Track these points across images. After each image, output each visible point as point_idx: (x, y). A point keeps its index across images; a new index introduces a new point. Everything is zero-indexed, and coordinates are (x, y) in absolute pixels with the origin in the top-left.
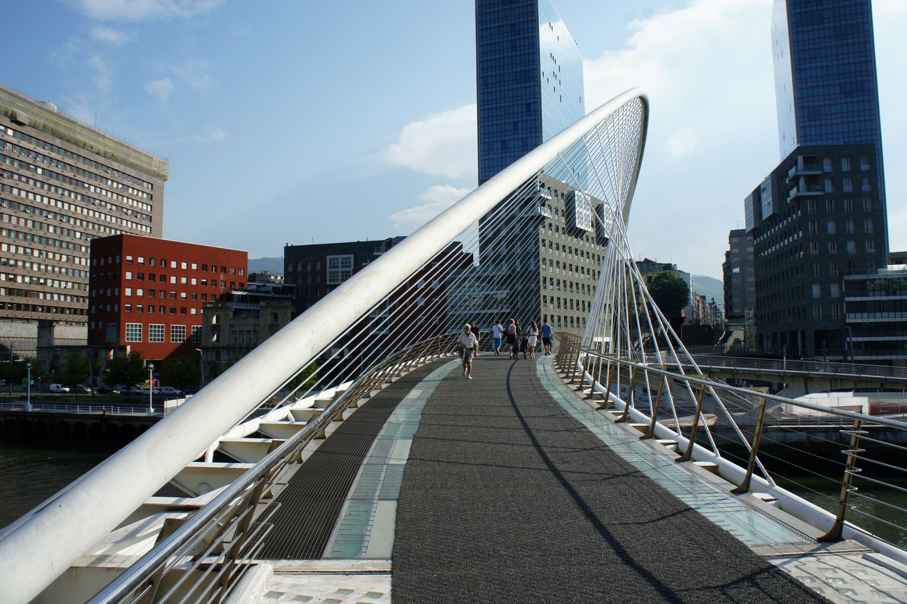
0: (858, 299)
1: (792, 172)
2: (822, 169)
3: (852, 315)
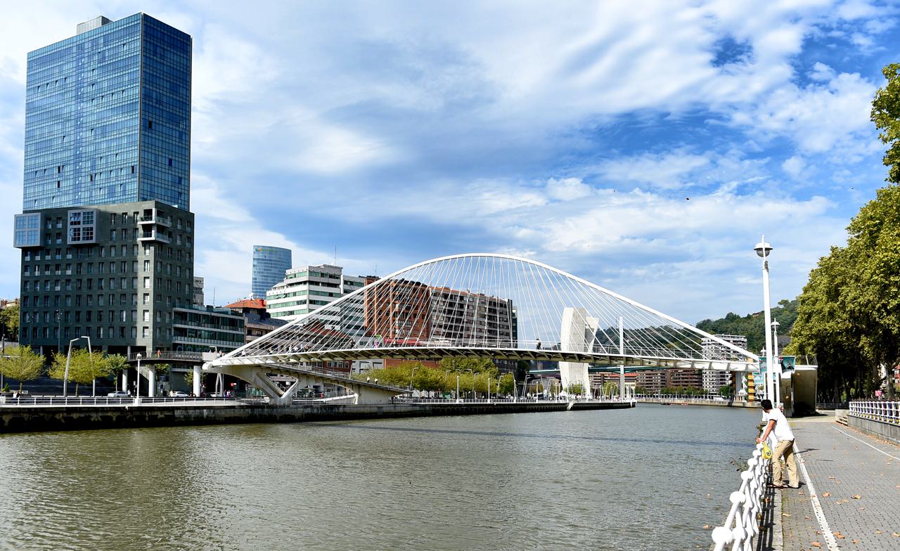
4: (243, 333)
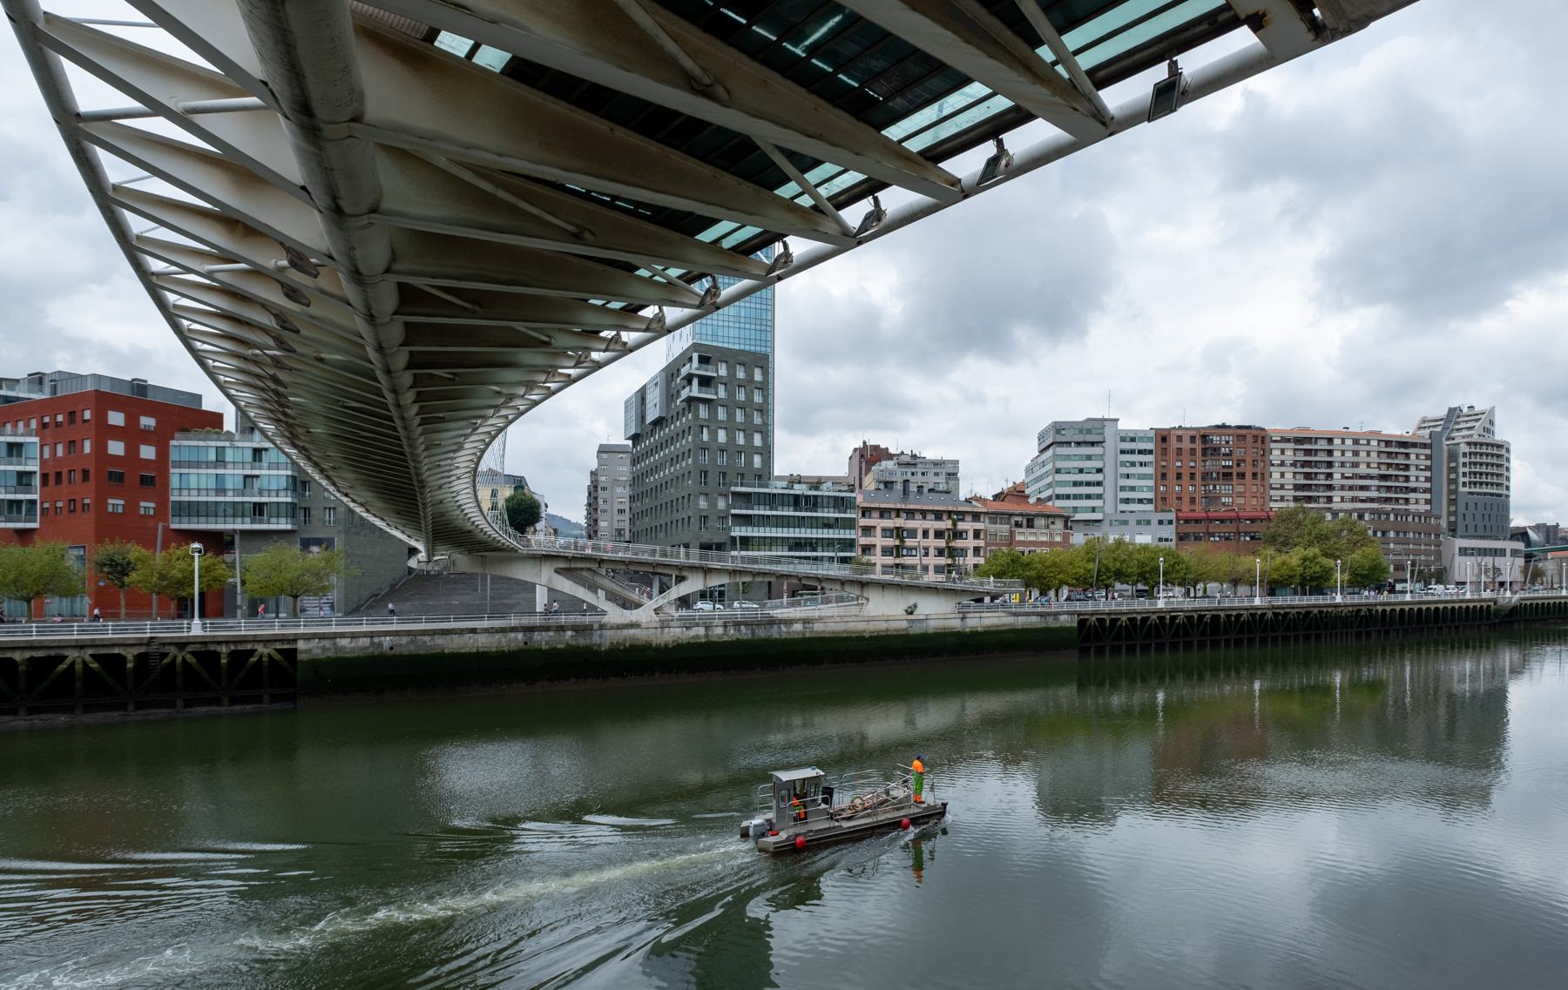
0: (744, 512)
1: (684, 371)
2: (717, 372)
3: (737, 528)
4: (853, 516)
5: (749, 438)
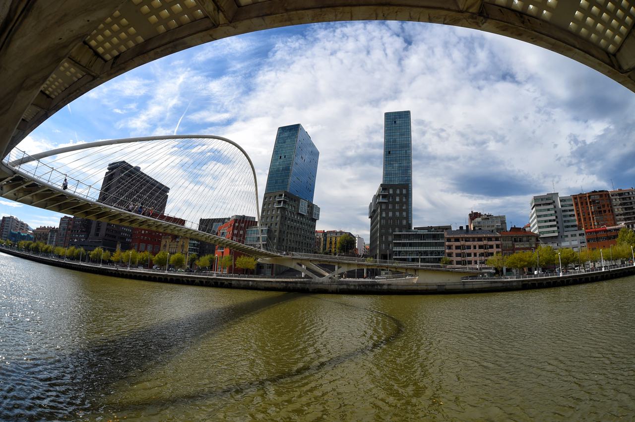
0: (398, 241)
3: (395, 248)
4: (443, 241)
5: (401, 214)
